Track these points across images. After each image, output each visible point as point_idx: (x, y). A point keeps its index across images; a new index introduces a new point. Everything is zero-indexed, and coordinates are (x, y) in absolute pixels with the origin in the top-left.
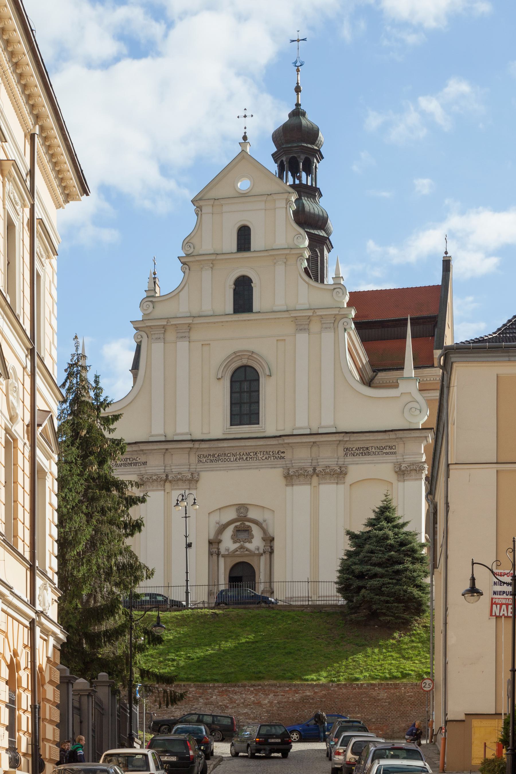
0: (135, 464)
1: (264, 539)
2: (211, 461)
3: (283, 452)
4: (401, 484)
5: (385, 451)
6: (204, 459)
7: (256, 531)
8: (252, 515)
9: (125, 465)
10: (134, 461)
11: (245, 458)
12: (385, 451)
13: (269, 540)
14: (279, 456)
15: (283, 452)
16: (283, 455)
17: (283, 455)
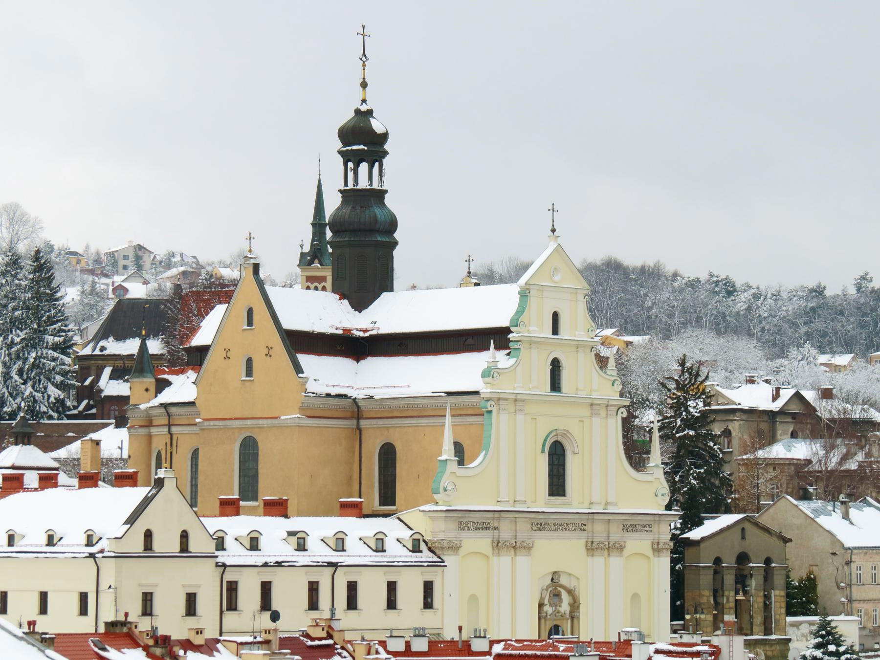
0: (489, 528)
1: (570, 605)
2: (540, 530)
3: (585, 525)
4: (656, 559)
5: (646, 529)
6: (535, 527)
7: (565, 597)
8: (564, 581)
9: (482, 529)
10: (488, 526)
11: (561, 528)
12: (646, 529)
13: (575, 606)
14: (582, 528)
15: (585, 525)
16: (584, 527)
17: (584, 527)
